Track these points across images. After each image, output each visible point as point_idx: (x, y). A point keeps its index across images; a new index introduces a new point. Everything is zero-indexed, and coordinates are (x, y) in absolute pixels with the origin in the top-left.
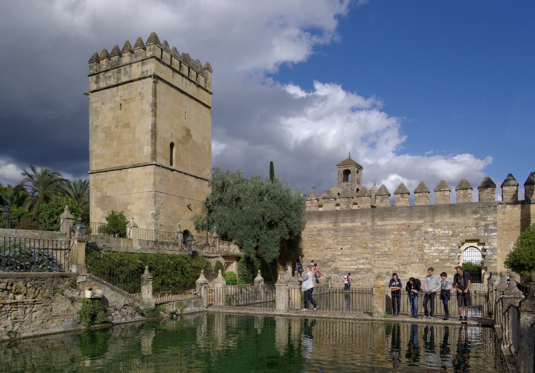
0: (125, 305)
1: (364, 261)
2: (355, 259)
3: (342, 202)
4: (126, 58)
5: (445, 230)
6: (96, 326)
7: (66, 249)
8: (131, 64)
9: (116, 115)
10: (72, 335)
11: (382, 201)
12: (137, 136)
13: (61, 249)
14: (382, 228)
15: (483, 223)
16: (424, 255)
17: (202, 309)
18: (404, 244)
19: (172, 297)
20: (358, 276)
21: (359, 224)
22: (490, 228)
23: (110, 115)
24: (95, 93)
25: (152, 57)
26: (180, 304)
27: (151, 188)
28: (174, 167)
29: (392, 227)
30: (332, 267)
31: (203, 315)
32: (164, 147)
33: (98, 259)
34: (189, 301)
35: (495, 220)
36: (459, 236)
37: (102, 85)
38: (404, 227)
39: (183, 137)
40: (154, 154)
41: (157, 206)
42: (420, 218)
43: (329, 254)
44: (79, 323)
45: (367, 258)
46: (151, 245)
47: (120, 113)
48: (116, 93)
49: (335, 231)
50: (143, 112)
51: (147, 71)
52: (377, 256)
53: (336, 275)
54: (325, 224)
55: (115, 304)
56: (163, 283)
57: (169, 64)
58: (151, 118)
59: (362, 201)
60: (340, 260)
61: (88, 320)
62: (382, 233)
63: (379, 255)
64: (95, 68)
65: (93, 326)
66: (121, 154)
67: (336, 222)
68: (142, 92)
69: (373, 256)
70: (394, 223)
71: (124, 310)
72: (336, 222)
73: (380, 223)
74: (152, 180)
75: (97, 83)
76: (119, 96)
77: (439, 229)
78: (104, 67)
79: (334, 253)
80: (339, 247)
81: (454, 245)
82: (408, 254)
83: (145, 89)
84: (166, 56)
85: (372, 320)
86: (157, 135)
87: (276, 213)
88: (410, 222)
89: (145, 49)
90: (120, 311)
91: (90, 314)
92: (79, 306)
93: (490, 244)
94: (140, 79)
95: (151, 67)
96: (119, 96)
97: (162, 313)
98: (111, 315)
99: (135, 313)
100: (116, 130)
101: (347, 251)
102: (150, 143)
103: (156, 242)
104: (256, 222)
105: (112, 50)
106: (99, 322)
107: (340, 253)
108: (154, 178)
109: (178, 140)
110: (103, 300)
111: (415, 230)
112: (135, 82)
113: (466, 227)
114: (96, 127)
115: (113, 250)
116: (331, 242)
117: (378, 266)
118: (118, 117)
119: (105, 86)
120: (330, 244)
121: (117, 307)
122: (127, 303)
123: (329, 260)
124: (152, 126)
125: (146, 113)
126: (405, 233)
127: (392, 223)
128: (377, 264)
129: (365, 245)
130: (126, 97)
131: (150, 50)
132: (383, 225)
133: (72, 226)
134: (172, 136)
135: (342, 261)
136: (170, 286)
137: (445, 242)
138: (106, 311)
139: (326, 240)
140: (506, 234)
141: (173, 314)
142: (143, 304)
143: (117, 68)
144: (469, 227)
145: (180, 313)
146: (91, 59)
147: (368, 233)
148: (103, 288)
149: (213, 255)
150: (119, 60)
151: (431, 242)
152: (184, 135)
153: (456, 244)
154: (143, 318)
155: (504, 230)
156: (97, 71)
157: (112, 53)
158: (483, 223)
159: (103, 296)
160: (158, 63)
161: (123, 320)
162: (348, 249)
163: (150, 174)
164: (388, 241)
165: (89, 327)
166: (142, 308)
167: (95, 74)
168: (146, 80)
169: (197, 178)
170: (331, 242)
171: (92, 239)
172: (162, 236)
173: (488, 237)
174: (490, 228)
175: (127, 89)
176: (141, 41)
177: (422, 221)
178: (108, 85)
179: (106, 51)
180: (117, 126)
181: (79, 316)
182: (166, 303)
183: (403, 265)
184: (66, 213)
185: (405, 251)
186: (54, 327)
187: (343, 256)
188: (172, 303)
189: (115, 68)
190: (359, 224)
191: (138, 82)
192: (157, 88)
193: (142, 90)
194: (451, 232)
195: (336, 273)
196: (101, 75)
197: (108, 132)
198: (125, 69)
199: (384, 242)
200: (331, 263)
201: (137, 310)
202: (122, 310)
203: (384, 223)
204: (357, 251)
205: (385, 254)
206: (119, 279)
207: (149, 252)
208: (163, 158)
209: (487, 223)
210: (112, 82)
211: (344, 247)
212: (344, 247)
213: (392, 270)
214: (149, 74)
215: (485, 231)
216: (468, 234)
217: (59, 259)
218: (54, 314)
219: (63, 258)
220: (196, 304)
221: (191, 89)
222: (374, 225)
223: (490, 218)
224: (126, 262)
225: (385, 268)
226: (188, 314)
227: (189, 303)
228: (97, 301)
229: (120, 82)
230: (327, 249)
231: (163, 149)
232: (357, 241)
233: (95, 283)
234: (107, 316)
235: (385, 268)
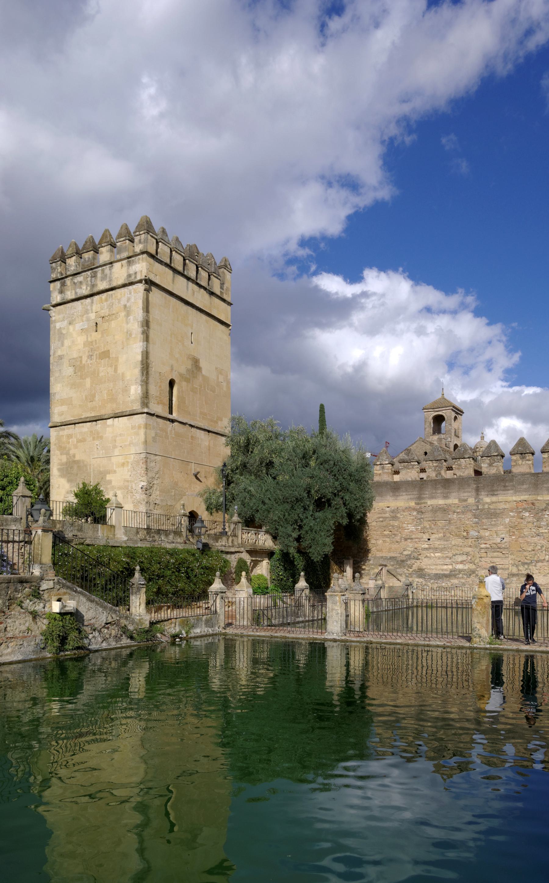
0: (107, 624)
1: (464, 558)
2: (450, 555)
3: (430, 467)
4: (105, 255)
6: (67, 653)
7: (21, 542)
8: (111, 263)
9: (89, 339)
10: (34, 667)
12: (120, 371)
13: (14, 542)
14: (491, 507)
17: (217, 630)
18: (526, 532)
19: (175, 613)
20: (455, 581)
21: (456, 501)
23: (81, 340)
24: (59, 307)
25: (143, 253)
26: (185, 623)
27: (140, 448)
28: (175, 416)
29: (507, 506)
30: (415, 567)
31: (219, 640)
32: (160, 387)
33: (66, 554)
34: (198, 618)
37: (70, 295)
38: (525, 506)
39: (188, 370)
40: (146, 397)
41: (151, 474)
43: (410, 547)
44: (44, 648)
45: (467, 554)
46: (141, 535)
47: (95, 336)
48: (89, 308)
49: (420, 512)
50: (129, 334)
51: (136, 273)
52: (483, 551)
53: (421, 580)
54: (403, 501)
55: (93, 621)
56: (159, 592)
57: (168, 261)
58: (141, 344)
59: (460, 465)
60: (426, 557)
61: (56, 644)
62: (491, 515)
63: (487, 548)
64: (59, 270)
65: (62, 653)
66: (97, 398)
67: (420, 498)
68: (128, 305)
69: (478, 550)
71: (106, 631)
72: (420, 498)
73: (487, 500)
74: (142, 437)
75: (61, 292)
76: (94, 311)
78: (72, 268)
79: (416, 546)
80: (426, 537)
83: (132, 300)
84: (164, 250)
85: (470, 648)
86: (150, 369)
87: (327, 485)
89: (132, 241)
90: (100, 632)
91: (59, 636)
92: (43, 624)
94: (124, 286)
95: (142, 267)
96: (94, 311)
97: (159, 635)
98: (87, 638)
99: (122, 636)
100: (89, 362)
101: (438, 543)
102: (139, 381)
103: (148, 529)
104: (297, 500)
105: (84, 243)
106: (71, 648)
107: (427, 546)
108: (146, 434)
109: (181, 375)
110: (76, 615)
112: (118, 290)
114: (61, 357)
115: (88, 542)
116: (413, 529)
118: (92, 342)
119: (73, 297)
120: (412, 531)
121: (96, 626)
122: (110, 620)
123: (409, 557)
124: (142, 355)
125: (133, 336)
128: (483, 563)
129: (465, 534)
130: (105, 312)
131: (140, 242)
133: (29, 507)
134: (172, 369)
135: (430, 558)
136: (170, 595)
138: (80, 632)
139: (405, 525)
141: (174, 637)
142: (133, 622)
143: (92, 269)
145: (185, 635)
146: (53, 257)
147: (469, 515)
148: (77, 598)
149: (233, 550)
150: (94, 258)
152: (190, 367)
154: (133, 643)
156: (62, 274)
157: (84, 248)
159: (77, 609)
160: (151, 260)
161: (104, 645)
162: (439, 539)
163: (139, 427)
164: (501, 527)
165: (57, 654)
166: (131, 628)
167: (59, 280)
168: (134, 287)
169: (209, 431)
170: (413, 529)
171: (58, 526)
172: (158, 521)
175: (106, 300)
176: (127, 229)
178: (79, 296)
179: (76, 244)
180: (90, 357)
181: (43, 638)
182: (165, 621)
183: (524, 564)
184: (21, 489)
185: (528, 543)
186: (10, 654)
187: (431, 551)
188: (172, 621)
189: (88, 270)
190: (456, 501)
191: (123, 290)
192: (150, 299)
193: (128, 302)
195: (420, 576)
196: (68, 281)
197: (79, 367)
198: (103, 271)
199: (495, 529)
200: (413, 561)
201: (124, 630)
202: (103, 630)
203: (494, 499)
204: (453, 543)
206: (95, 585)
207: (139, 545)
208: (158, 403)
210: (84, 290)
211: (433, 537)
212: (433, 537)
213: (506, 572)
214: (139, 278)
217: (10, 555)
218: (9, 635)
219: (16, 554)
220: (209, 623)
221: (200, 298)
222: (478, 502)
224: (106, 559)
226: (197, 637)
227: (198, 620)
228: (68, 617)
229: (96, 290)
230: (406, 539)
231: (158, 389)
232: (453, 527)
233: (65, 591)
234: (82, 639)
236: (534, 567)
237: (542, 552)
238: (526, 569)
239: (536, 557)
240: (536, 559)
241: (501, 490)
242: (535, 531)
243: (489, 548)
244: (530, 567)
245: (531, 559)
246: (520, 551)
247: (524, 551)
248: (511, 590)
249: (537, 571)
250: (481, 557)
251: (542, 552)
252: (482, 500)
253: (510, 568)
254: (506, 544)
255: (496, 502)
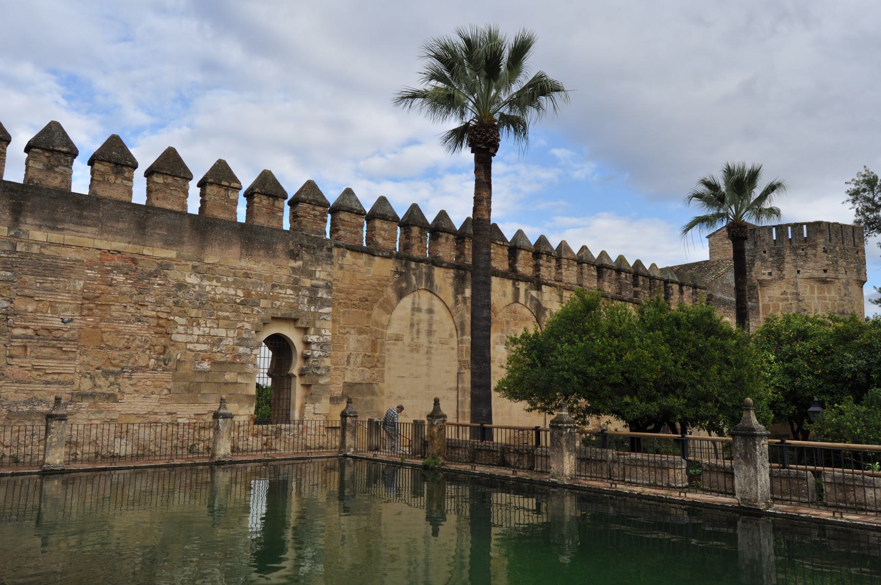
5: (227, 285)
11: (50, 168)
14: (46, 252)
15: (307, 282)
16: (171, 349)
18: (115, 311)
22: (319, 295)
35: (329, 278)
36: (258, 305)
42: (168, 244)
52: (17, 342)
62: (46, 267)
63: (26, 337)
70: (88, 242)
73: (39, 235)
77: (214, 283)
81: (248, 326)
82: (122, 343)
88: (138, 248)
93: (318, 332)
111: (150, 275)
113: (274, 286)
117: (20, 377)
126: (121, 278)
127: (82, 242)
128: (16, 369)
132: (52, 244)
137: (226, 318)
140: (344, 313)
144: (281, 287)
151: (194, 313)
153: (252, 324)
155: (340, 304)
158: (307, 282)
173: (317, 316)
174: (319, 295)
177: (171, 254)
183: (106, 374)
185: (118, 332)
194: (240, 293)
203: (55, 237)
205: (47, 338)
209: (315, 282)
213: (68, 390)
215: (313, 300)
216: (278, 303)
223: (321, 273)
225: (48, 383)
235: (48, 383)
236: (126, 380)
237: (144, 352)
238: (112, 384)
239: (132, 361)
240: (130, 365)
241: (71, 222)
242: (133, 310)
243: (31, 337)
244: (120, 380)
245: (123, 365)
246: (101, 348)
247: (110, 348)
248: (75, 427)
249: (132, 389)
250: (11, 357)
251: (144, 352)
252: (26, 233)
253: (77, 382)
254: (73, 332)
255: (59, 245)
